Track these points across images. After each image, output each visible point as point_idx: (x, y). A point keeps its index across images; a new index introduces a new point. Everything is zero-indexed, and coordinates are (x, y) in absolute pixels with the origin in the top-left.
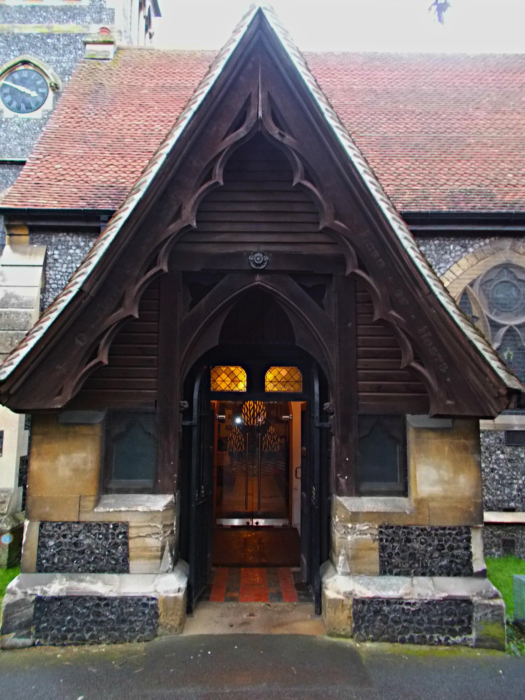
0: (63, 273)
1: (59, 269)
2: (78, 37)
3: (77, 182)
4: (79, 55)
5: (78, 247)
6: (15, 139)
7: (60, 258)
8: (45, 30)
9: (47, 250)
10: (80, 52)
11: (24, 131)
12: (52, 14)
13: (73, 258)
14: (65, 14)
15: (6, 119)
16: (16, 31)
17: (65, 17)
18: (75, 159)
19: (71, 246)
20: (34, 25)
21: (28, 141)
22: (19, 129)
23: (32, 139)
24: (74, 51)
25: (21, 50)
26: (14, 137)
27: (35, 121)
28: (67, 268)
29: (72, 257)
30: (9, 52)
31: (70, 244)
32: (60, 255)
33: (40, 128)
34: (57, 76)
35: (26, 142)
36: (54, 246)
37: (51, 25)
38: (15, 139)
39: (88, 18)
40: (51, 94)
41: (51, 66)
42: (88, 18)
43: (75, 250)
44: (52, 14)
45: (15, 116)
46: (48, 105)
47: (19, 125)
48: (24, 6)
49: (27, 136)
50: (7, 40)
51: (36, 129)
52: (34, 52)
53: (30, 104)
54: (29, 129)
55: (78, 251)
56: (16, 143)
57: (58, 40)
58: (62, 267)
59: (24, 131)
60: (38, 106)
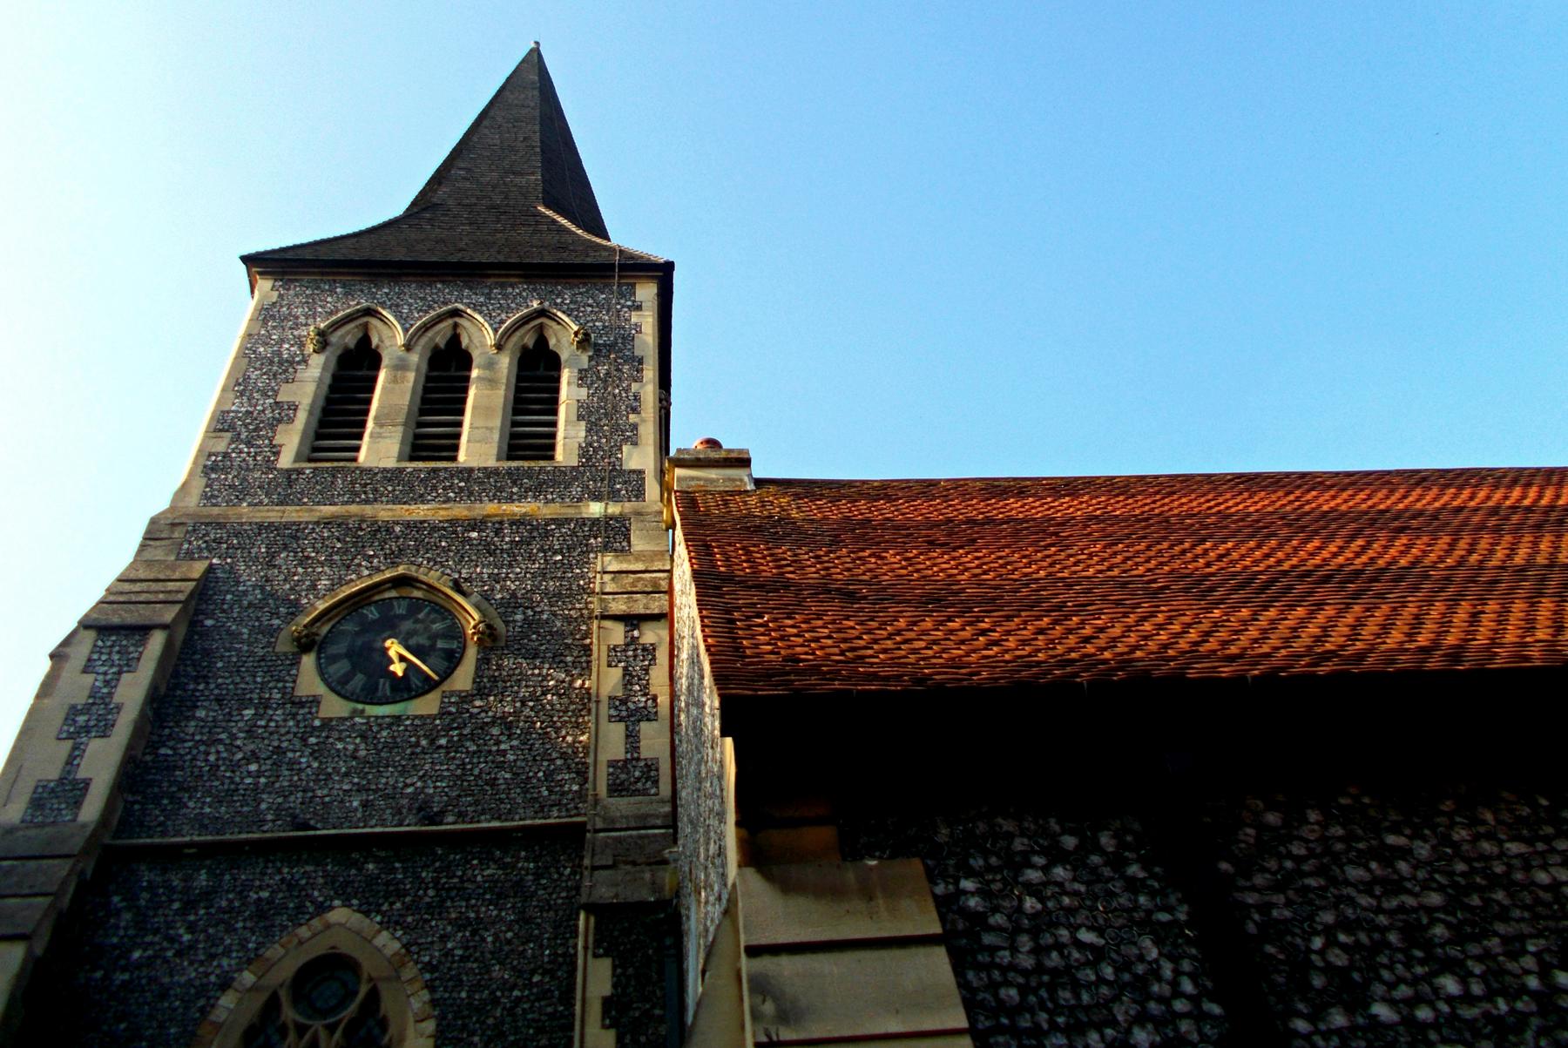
5: (1057, 856)
6: (347, 774)
7: (996, 910)
11: (379, 752)
13: (1050, 904)
15: (327, 723)
19: (1025, 854)
20: (433, 505)
21: (389, 778)
22: (363, 746)
23: (404, 772)
25: (393, 559)
26: (344, 769)
27: (417, 722)
29: (1042, 900)
30: (356, 561)
31: (1019, 844)
32: (983, 893)
33: (432, 742)
34: (491, 610)
35: (384, 780)
39: (576, 490)
44: (482, 483)
47: (364, 737)
48: (408, 470)
49: (387, 766)
51: (417, 744)
52: (429, 560)
54: (392, 746)
55: (1060, 872)
56: (346, 787)
57: (498, 532)
58: (1014, 950)
59: (379, 752)
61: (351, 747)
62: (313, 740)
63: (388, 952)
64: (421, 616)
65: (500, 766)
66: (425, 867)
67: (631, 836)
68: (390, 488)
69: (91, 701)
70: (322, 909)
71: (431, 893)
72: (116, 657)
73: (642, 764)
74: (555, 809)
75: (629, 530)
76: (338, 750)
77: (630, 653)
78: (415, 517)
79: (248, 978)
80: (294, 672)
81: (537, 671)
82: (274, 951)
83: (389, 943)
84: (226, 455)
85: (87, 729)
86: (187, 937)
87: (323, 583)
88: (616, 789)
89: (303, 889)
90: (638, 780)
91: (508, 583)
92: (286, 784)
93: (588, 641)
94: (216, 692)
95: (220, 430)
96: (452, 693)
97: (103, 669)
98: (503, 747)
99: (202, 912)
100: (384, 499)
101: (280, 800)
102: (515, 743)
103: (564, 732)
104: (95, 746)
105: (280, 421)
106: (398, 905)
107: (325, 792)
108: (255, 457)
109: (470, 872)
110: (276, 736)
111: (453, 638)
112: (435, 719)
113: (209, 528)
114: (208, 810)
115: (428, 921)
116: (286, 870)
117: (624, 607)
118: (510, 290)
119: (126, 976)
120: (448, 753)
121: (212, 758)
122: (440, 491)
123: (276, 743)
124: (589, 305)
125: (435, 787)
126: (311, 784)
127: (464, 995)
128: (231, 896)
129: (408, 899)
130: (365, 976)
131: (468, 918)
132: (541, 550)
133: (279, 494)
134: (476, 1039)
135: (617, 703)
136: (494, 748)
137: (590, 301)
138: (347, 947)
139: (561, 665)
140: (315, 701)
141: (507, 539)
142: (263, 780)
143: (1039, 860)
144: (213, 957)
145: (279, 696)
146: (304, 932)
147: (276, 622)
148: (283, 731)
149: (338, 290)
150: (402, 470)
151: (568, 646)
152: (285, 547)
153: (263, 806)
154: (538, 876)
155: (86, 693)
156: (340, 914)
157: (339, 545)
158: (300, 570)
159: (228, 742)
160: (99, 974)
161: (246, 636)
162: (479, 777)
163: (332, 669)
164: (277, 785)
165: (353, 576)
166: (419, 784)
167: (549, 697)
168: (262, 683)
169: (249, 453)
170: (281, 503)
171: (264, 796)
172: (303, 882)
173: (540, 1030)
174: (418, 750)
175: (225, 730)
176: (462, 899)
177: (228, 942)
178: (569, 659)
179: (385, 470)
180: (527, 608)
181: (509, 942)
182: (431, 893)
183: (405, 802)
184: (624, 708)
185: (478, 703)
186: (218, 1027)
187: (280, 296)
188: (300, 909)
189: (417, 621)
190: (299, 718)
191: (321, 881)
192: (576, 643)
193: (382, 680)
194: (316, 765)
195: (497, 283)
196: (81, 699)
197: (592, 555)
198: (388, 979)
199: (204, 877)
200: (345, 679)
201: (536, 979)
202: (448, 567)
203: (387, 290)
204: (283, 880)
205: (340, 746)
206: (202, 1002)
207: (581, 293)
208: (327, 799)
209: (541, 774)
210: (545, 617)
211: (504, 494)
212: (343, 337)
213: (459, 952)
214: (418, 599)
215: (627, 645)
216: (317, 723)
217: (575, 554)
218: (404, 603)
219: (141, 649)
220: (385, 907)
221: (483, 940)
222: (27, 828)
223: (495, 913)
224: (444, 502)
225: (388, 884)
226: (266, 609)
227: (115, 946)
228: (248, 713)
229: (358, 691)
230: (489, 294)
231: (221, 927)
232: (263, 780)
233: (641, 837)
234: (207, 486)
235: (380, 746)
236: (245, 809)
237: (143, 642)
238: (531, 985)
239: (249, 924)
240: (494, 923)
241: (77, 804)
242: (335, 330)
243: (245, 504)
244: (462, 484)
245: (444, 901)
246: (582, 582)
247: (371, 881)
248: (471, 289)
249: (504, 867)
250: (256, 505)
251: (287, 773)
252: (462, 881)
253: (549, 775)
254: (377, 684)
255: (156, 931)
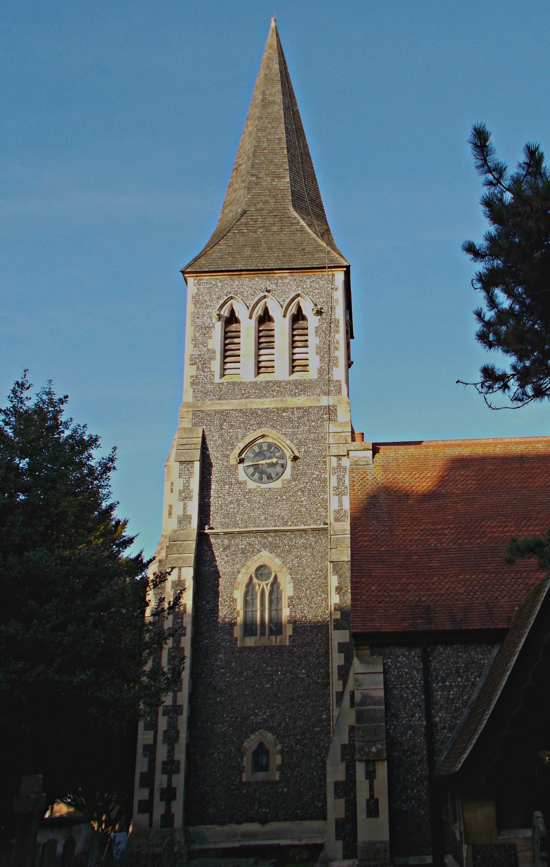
0: (395, 676)
1: (393, 673)
2: (310, 410)
3: (392, 602)
4: (313, 426)
5: (404, 656)
6: (259, 508)
8: (280, 405)
9: (383, 660)
10: (313, 424)
12: (284, 388)
14: (296, 388)
16: (254, 406)
17: (297, 391)
18: (382, 579)
22: (262, 499)
24: (308, 422)
25: (260, 425)
26: (257, 507)
27: (276, 490)
28: (398, 672)
30: (248, 427)
36: (387, 656)
37: (284, 399)
38: (259, 508)
39: (318, 391)
40: (289, 464)
41: (288, 438)
42: (318, 391)
43: (402, 658)
44: (284, 388)
45: (257, 486)
46: (287, 474)
48: (259, 382)
50: (246, 416)
53: (271, 474)
55: (404, 659)
56: (260, 513)
57: (293, 413)
58: (394, 671)
60: (279, 476)
61: (258, 499)
62: (247, 497)
63: (279, 565)
64: (272, 450)
65: (301, 506)
66: (285, 539)
67: (341, 537)
68: (254, 391)
69: (184, 488)
70: (259, 551)
71: (287, 547)
72: (187, 472)
73: (343, 511)
74: (319, 521)
75: (336, 411)
76: (255, 500)
77: (339, 470)
78: (264, 407)
79: (243, 570)
80: (237, 472)
81: (310, 471)
82: (249, 563)
83: (278, 561)
84: (196, 377)
85: (186, 498)
86: (226, 559)
87: (240, 436)
88: (337, 520)
89: (253, 545)
90: (342, 516)
91: (298, 435)
92: (242, 511)
93: (325, 459)
94: (216, 479)
95: (192, 364)
96: (285, 480)
97: (184, 477)
98: (302, 499)
99: (228, 551)
100: (252, 396)
101: (242, 517)
102: (306, 498)
103: (319, 495)
104: (189, 503)
105: (211, 359)
106: (279, 550)
107: (254, 514)
108: (206, 377)
109: (297, 541)
110: (236, 495)
111: (283, 459)
112: (281, 489)
113: (199, 413)
114: (223, 520)
115: (287, 555)
116: (247, 539)
117: (336, 451)
118: (285, 281)
119: (213, 569)
120: (286, 501)
121: (220, 502)
122: (271, 392)
123: (237, 498)
124: (318, 289)
125: (284, 513)
126: (249, 512)
127: (299, 576)
128: (235, 547)
129: (281, 548)
130: (273, 571)
131: (298, 555)
132: (308, 420)
133: (218, 395)
134: (304, 588)
135: (335, 489)
136: (299, 500)
137: (317, 286)
138: (266, 563)
139: (317, 469)
140: (245, 482)
141: (296, 416)
142: (236, 510)
143: (401, 657)
144: (234, 564)
145: (234, 481)
146: (255, 558)
147: (228, 452)
148: (238, 493)
149: (219, 284)
150: (256, 383)
151: (319, 462)
152: (225, 421)
153: (237, 519)
154: (316, 543)
155: (182, 486)
156: (265, 553)
157: (241, 419)
158: (231, 431)
159: (223, 497)
160: (207, 568)
161: (220, 458)
162: (296, 510)
163: (248, 471)
164: (240, 512)
165: (248, 433)
166: (280, 512)
167: (314, 481)
168: (229, 476)
169: (204, 375)
170: (219, 399)
171: (237, 516)
172: (252, 543)
173: (320, 586)
174: (278, 500)
175: (222, 493)
176: (296, 549)
177: (237, 560)
178: (320, 466)
179: (251, 383)
180: (305, 446)
181: (310, 562)
182: (287, 547)
183: (276, 518)
184: (337, 491)
185: (293, 483)
186: (239, 583)
187: (198, 289)
188: (253, 551)
189: (271, 452)
190: (242, 488)
191: (257, 543)
192: (322, 460)
193: (264, 475)
194: (249, 505)
195: (279, 277)
196: (182, 488)
197: (325, 423)
198: (280, 572)
199: (226, 541)
200: (253, 475)
201: (318, 572)
202: (278, 429)
203: (237, 283)
204: (247, 542)
205: (255, 498)
206: (234, 577)
207: (313, 281)
208: (254, 517)
209: (314, 509)
210: (311, 449)
211: (293, 393)
212: (225, 312)
213: (297, 564)
214: (270, 443)
215: (338, 466)
216: (247, 490)
217: (319, 422)
218: (266, 445)
219: (193, 469)
220: (275, 551)
221: (303, 561)
222: (180, 530)
223: (305, 553)
224: (273, 397)
225: (275, 544)
226: (224, 447)
227: (209, 561)
228: (227, 486)
229: (257, 479)
230: (277, 282)
231: (234, 555)
232: (236, 510)
233: (344, 538)
234: (194, 392)
235: (267, 499)
236: (233, 520)
237: (192, 467)
238: (316, 574)
239: (241, 555)
240: (305, 556)
241: (190, 522)
242: (222, 309)
243: (208, 400)
244: (278, 389)
245: (291, 549)
246: (322, 435)
247: (271, 543)
248: (270, 280)
249: (306, 539)
250: (211, 400)
251: (241, 508)
252: (295, 544)
253: (316, 509)
254: (262, 477)
255: (218, 557)
